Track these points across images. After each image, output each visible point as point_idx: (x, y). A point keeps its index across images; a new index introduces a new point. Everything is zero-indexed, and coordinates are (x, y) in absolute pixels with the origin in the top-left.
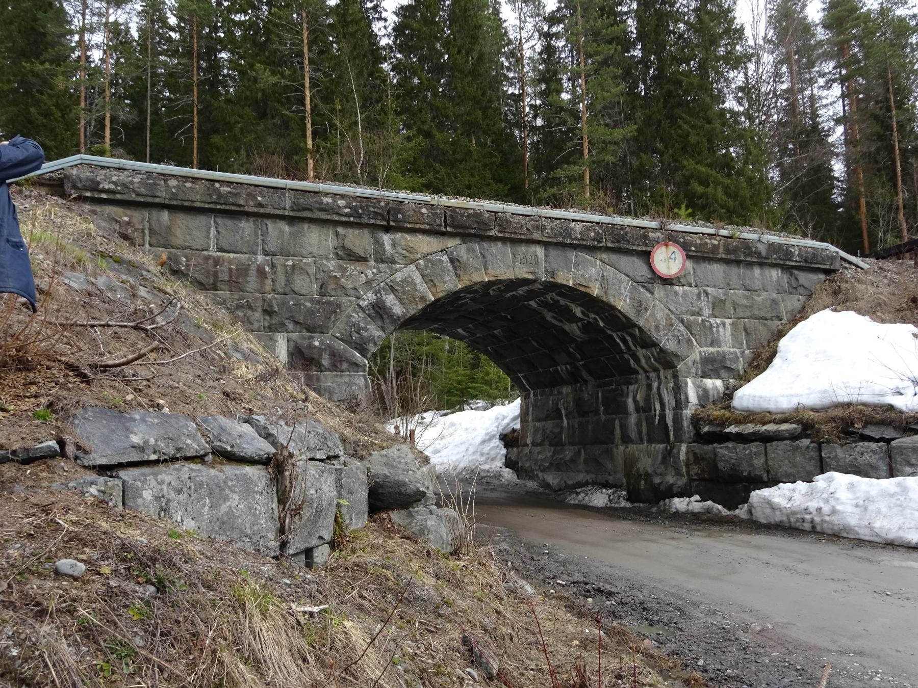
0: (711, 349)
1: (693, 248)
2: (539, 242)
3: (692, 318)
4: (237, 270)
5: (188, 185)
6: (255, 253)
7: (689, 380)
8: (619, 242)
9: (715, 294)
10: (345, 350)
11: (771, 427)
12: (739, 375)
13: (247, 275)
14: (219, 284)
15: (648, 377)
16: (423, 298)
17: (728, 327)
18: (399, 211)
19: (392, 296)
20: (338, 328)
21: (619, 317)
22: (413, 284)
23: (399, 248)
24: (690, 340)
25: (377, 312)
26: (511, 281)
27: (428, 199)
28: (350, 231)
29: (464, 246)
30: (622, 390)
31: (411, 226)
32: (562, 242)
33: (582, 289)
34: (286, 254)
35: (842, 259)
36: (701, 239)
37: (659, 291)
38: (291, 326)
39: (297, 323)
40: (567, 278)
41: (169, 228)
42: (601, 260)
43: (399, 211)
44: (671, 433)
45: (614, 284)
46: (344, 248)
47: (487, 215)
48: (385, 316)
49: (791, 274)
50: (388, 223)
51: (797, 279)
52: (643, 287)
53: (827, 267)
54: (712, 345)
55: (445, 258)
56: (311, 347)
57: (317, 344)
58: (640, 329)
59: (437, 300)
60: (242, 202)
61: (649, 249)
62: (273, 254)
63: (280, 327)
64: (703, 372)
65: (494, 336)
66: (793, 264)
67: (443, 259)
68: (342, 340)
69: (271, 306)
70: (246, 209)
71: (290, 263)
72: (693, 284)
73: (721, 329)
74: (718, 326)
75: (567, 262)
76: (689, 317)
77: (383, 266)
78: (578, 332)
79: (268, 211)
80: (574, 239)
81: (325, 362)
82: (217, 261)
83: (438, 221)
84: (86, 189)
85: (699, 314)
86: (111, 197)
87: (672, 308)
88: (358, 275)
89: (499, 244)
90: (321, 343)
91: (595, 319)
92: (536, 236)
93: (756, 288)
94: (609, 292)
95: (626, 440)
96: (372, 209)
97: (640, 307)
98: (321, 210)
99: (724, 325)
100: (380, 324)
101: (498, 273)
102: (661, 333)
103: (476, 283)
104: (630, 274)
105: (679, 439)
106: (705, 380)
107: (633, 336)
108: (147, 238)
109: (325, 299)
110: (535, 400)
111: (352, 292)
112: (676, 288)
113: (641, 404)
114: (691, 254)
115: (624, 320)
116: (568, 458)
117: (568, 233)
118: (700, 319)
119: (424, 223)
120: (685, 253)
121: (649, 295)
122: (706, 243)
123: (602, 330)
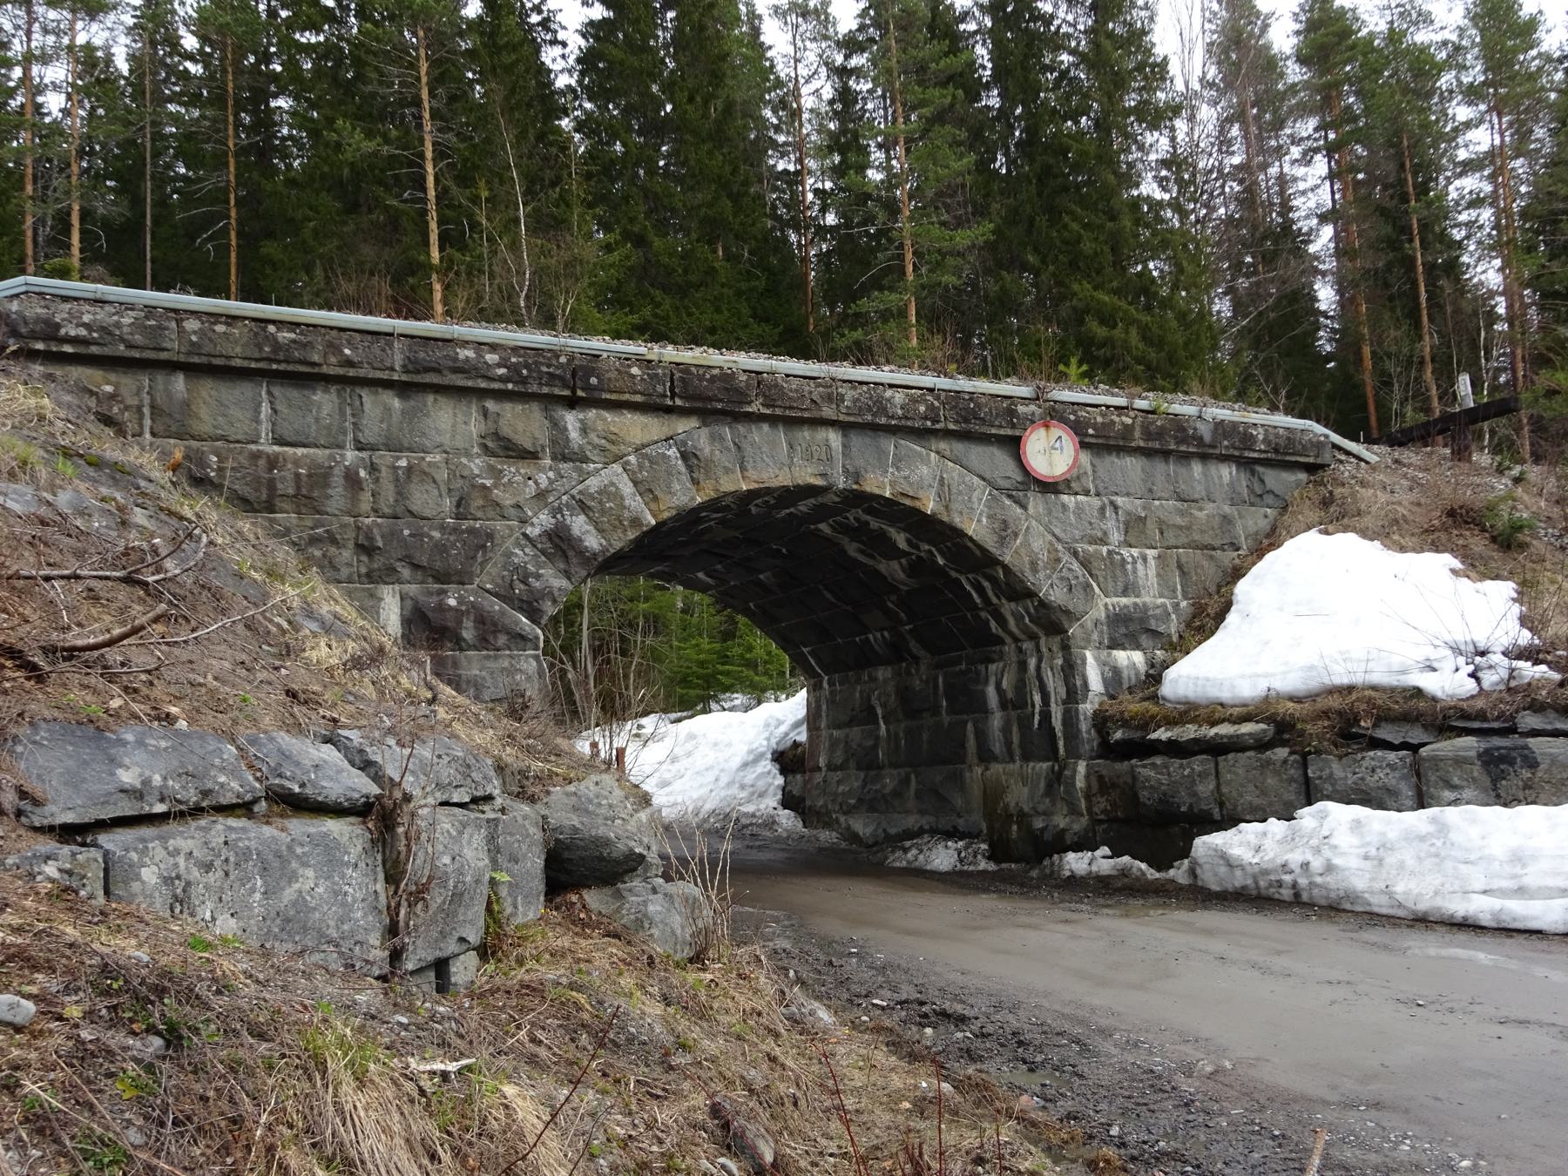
0: (1124, 601)
1: (1091, 431)
2: (832, 423)
3: (1091, 548)
4: (310, 476)
5: (220, 328)
6: (341, 447)
7: (1089, 655)
8: (967, 421)
9: (1129, 507)
10: (503, 613)
11: (1225, 729)
12: (1171, 644)
13: (327, 485)
14: (278, 503)
15: (1020, 650)
16: (636, 522)
17: (1152, 563)
18: (590, 371)
19: (582, 518)
20: (489, 576)
21: (968, 548)
22: (618, 497)
23: (593, 436)
24: (1089, 585)
25: (556, 546)
26: (786, 489)
27: (642, 350)
28: (508, 406)
29: (705, 431)
30: (978, 673)
31: (614, 397)
32: (871, 422)
33: (907, 502)
34: (395, 447)
35: (1335, 446)
36: (1103, 415)
37: (1036, 503)
38: (406, 572)
39: (416, 567)
40: (880, 483)
41: (187, 404)
42: (938, 453)
43: (590, 371)
44: (1061, 744)
45: (960, 493)
46: (497, 436)
47: (743, 378)
48: (571, 553)
49: (1253, 473)
50: (574, 392)
51: (1262, 481)
52: (1010, 497)
53: (1311, 460)
54: (1125, 593)
55: (673, 452)
56: (442, 608)
57: (452, 602)
58: (1006, 568)
59: (660, 525)
60: (316, 358)
61: (1017, 433)
62: (373, 448)
63: (387, 575)
64: (1111, 639)
65: (760, 584)
66: (1255, 455)
67: (670, 453)
68: (496, 595)
69: (371, 538)
70: (325, 369)
71: (403, 463)
72: (1093, 491)
73: (1140, 566)
74: (1134, 562)
75: (881, 454)
76: (1086, 547)
77: (564, 466)
78: (902, 576)
79: (362, 373)
80: (892, 417)
81: (468, 634)
82: (273, 462)
83: (660, 389)
84: (35, 336)
85: (1103, 541)
86: (81, 350)
87: (1057, 531)
88: (520, 482)
89: (766, 427)
90: (461, 600)
91: (930, 552)
92: (828, 412)
93: (1197, 496)
94: (954, 506)
95: (986, 756)
96: (545, 369)
97: (1005, 531)
98: (456, 370)
99: (1145, 559)
100: (562, 566)
101: (765, 476)
102: (1041, 575)
103: (726, 494)
104: (987, 476)
105: (1073, 753)
106: (1115, 652)
107: (993, 580)
108: (147, 422)
109: (465, 525)
110: (831, 692)
111: (513, 512)
112: (1065, 498)
113: (1010, 695)
114: (1088, 440)
115: (978, 552)
116: (887, 791)
117: (881, 406)
118: (1105, 549)
119: (636, 392)
121: (1019, 511)
122: (1113, 423)
123: (941, 571)
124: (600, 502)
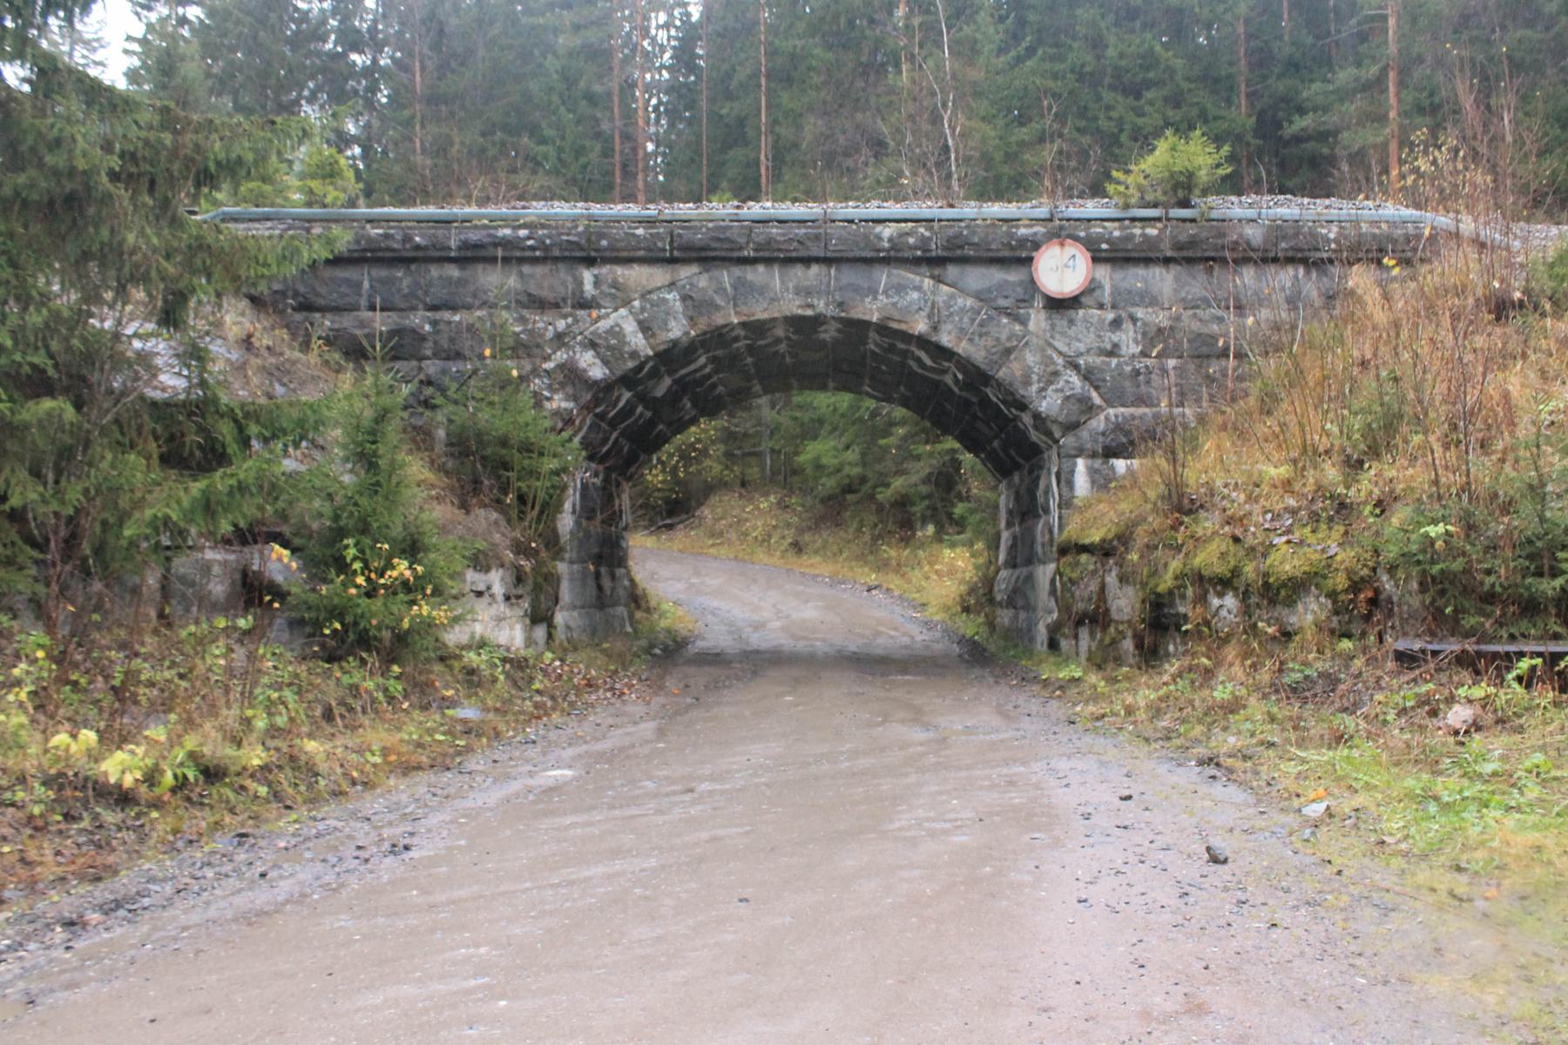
1: (1104, 246)
16: (634, 354)
23: (605, 288)
29: (706, 276)
33: (895, 325)
40: (871, 310)
52: (1009, 315)
77: (581, 313)
83: (660, 244)
87: (1056, 344)
102: (1034, 388)
118: (1114, 361)
120: (1088, 255)
122: (1134, 236)
124: (606, 339)
